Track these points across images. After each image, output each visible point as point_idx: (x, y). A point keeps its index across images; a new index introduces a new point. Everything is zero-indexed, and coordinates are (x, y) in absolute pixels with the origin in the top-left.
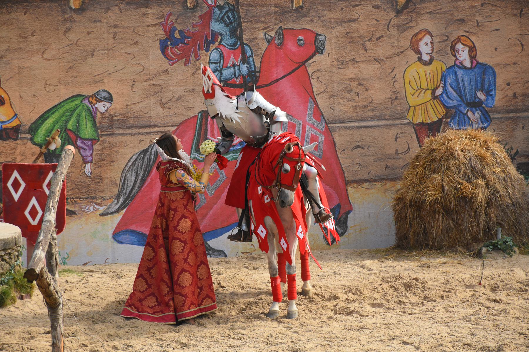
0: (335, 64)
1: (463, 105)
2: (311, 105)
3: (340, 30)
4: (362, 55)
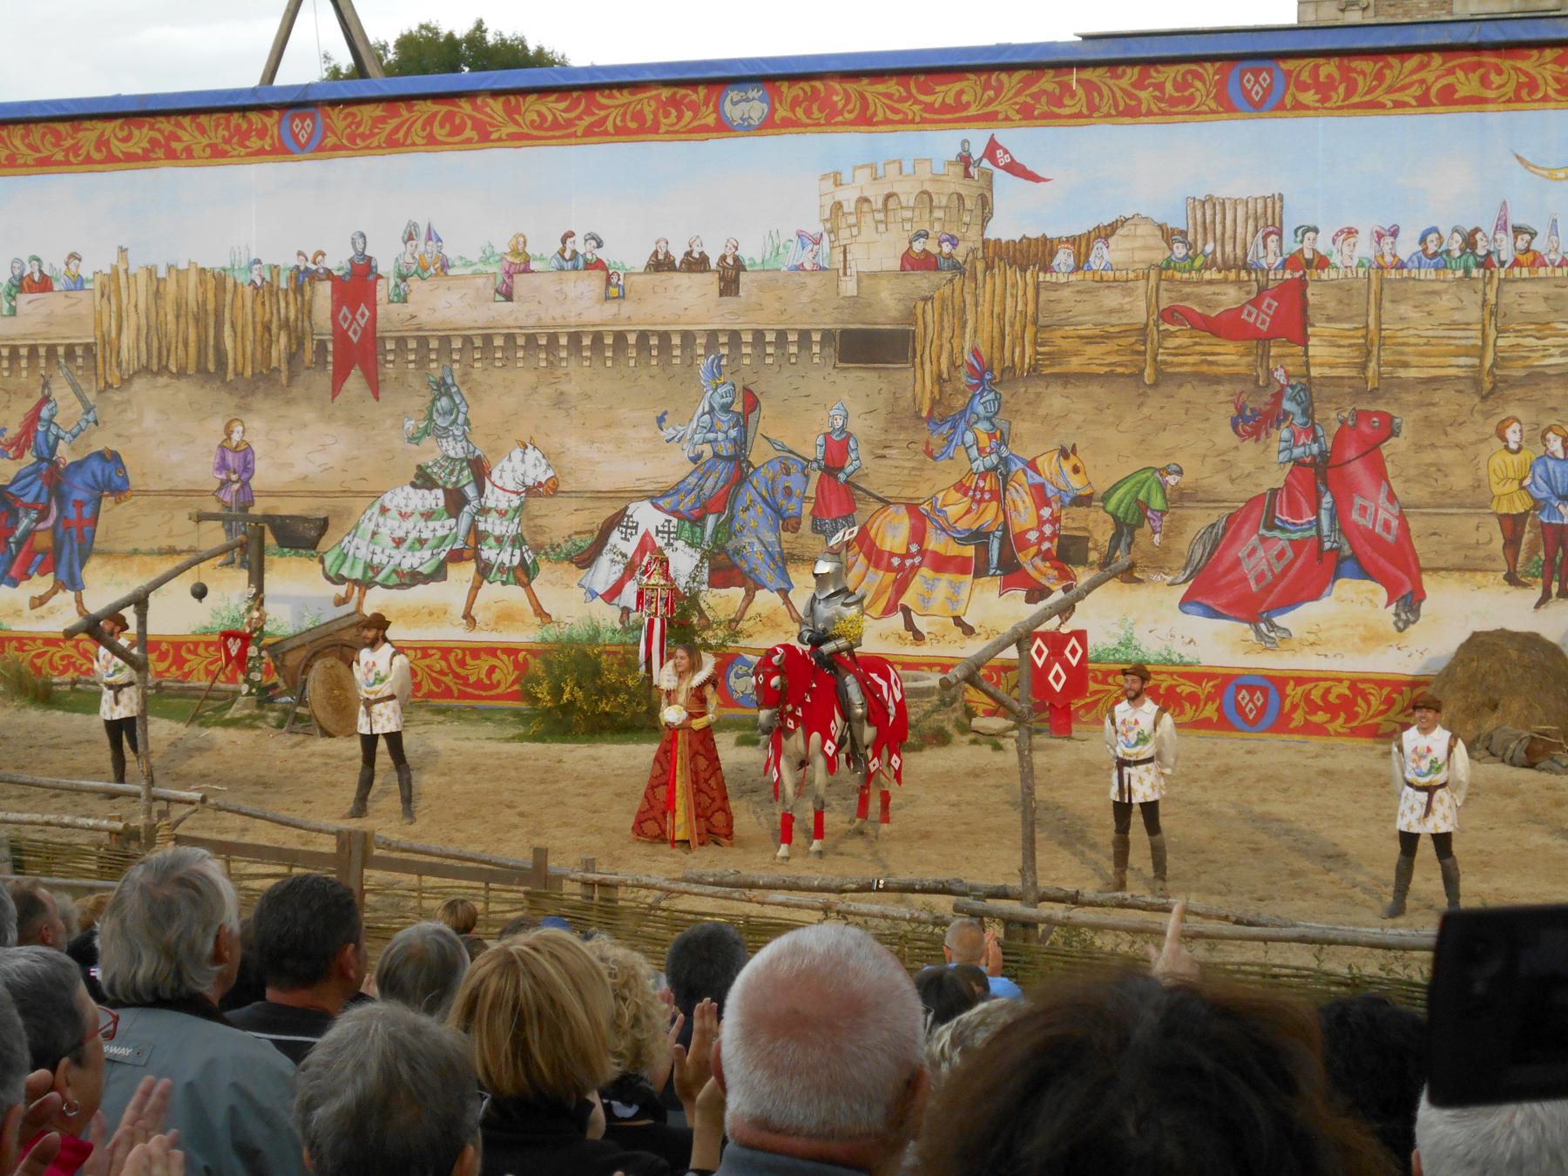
2: (1384, 488)
3: (1418, 413)
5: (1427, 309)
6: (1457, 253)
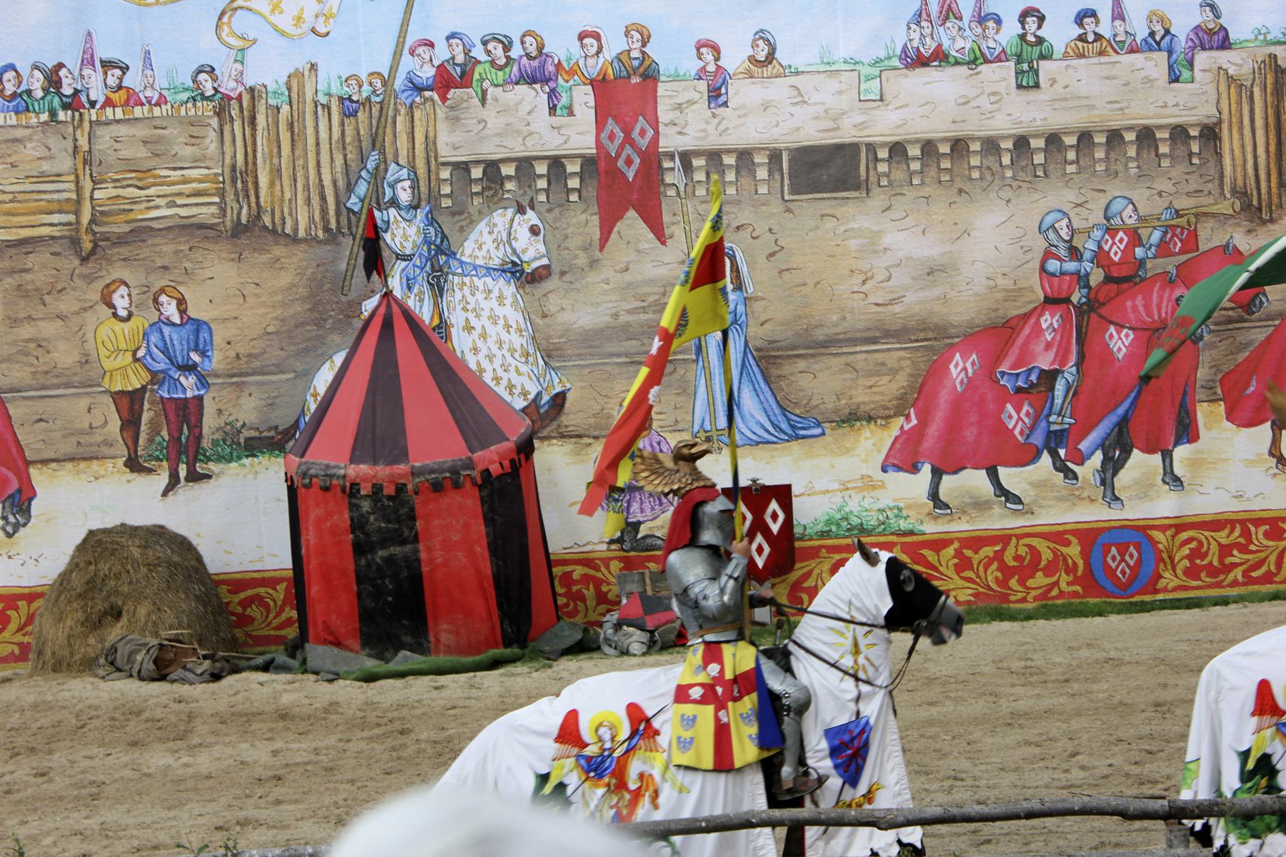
0: (8, 322)
1: (174, 369)
4: (40, 312)
5: (10, 160)
6: (39, 94)
